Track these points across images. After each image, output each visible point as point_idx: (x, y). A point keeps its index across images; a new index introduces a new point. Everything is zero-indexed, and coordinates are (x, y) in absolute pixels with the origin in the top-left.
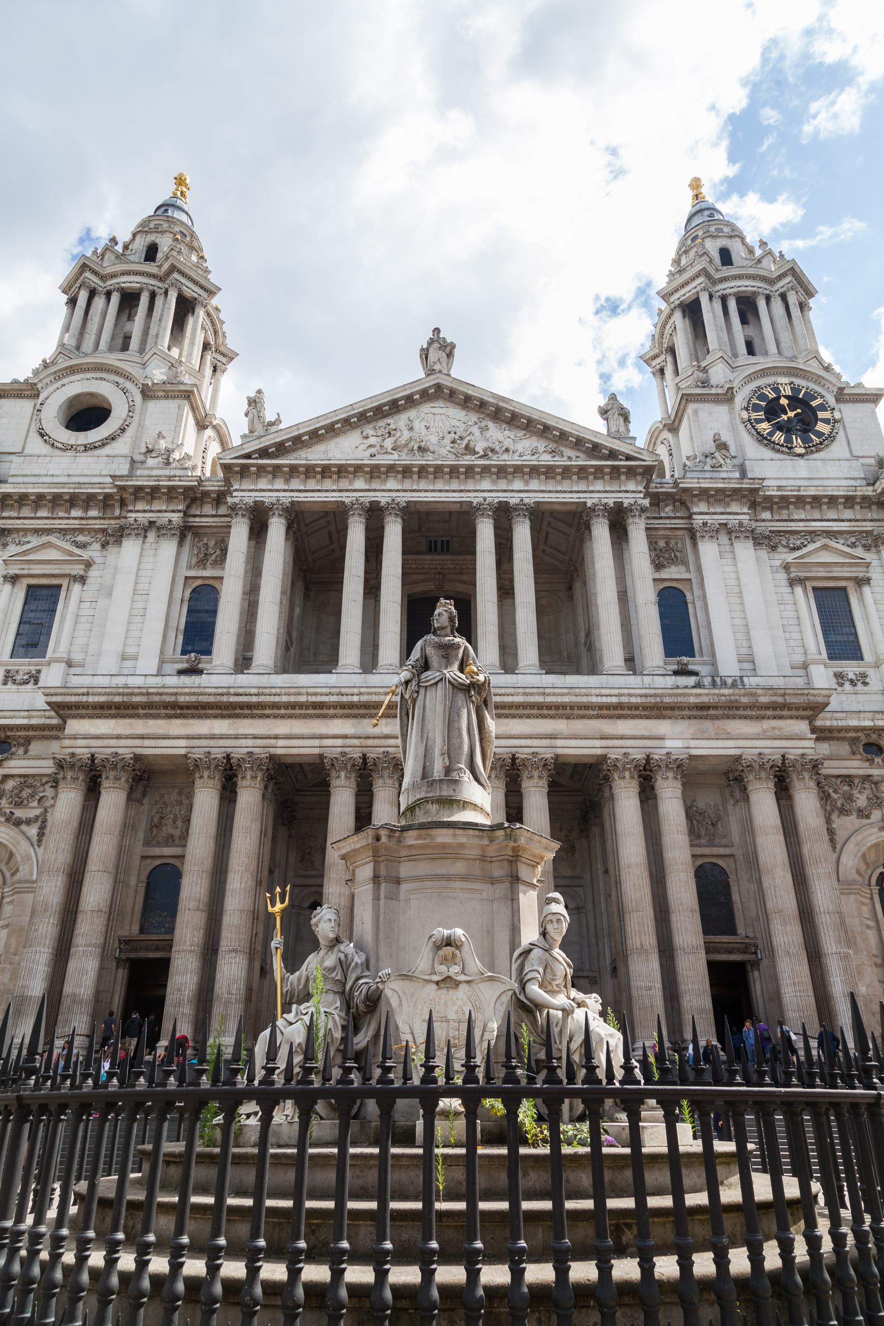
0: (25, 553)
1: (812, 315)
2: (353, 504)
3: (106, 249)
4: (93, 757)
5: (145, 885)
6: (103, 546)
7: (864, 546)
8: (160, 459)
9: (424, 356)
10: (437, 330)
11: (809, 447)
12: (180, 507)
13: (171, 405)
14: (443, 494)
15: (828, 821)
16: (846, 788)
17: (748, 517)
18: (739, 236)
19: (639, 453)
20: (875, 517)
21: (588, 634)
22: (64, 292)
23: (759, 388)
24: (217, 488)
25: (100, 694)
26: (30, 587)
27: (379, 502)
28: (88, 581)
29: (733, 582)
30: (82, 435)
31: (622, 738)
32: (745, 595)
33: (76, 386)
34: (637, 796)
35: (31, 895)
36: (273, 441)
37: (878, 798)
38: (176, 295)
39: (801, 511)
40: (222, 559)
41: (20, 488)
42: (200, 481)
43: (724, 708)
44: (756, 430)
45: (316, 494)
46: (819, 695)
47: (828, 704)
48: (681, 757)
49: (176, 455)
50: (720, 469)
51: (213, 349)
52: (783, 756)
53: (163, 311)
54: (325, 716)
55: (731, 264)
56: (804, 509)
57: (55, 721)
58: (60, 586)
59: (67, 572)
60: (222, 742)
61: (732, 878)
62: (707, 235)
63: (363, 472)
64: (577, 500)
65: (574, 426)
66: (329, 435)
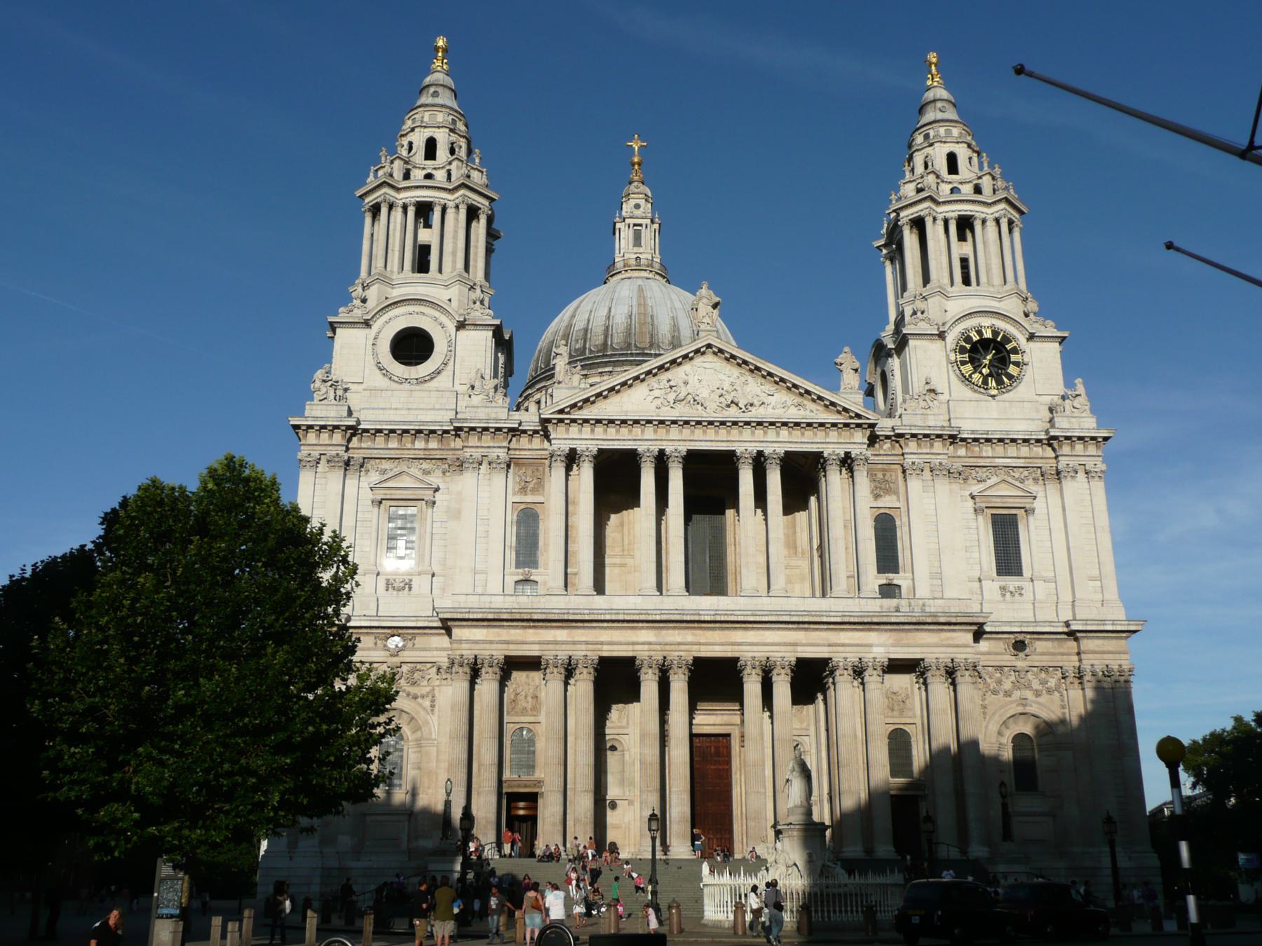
7: (1034, 479)
12: (505, 444)
14: (713, 444)
16: (998, 675)
17: (946, 457)
18: (965, 143)
24: (532, 428)
25: (477, 613)
30: (413, 368)
31: (843, 645)
33: (401, 320)
35: (435, 748)
36: (581, 398)
45: (616, 443)
48: (883, 660)
50: (928, 411)
52: (952, 660)
60: (564, 647)
61: (913, 739)
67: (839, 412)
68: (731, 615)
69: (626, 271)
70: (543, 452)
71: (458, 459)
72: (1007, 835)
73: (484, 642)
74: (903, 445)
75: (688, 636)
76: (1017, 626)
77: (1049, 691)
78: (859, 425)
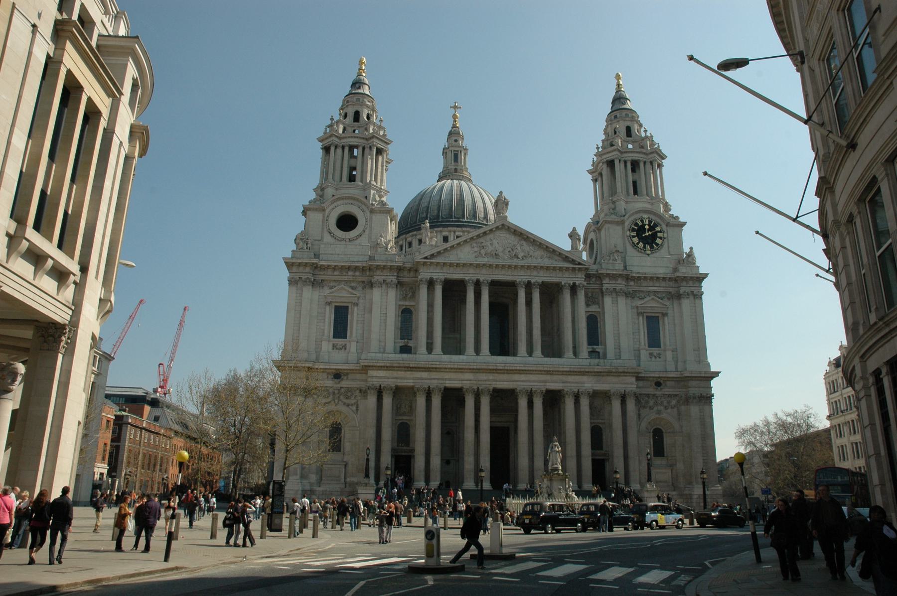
0: (332, 293)
1: (664, 169)
6: (363, 289)
7: (668, 298)
10: (501, 193)
14: (505, 276)
15: (639, 411)
22: (320, 141)
26: (336, 306)
28: (360, 305)
30: (347, 233)
31: (570, 383)
45: (454, 275)
54: (463, 372)
55: (631, 137)
60: (426, 381)
67: (569, 262)
69: (449, 176)
70: (416, 279)
71: (371, 281)
72: (649, 480)
73: (384, 377)
75: (491, 377)
78: (580, 269)
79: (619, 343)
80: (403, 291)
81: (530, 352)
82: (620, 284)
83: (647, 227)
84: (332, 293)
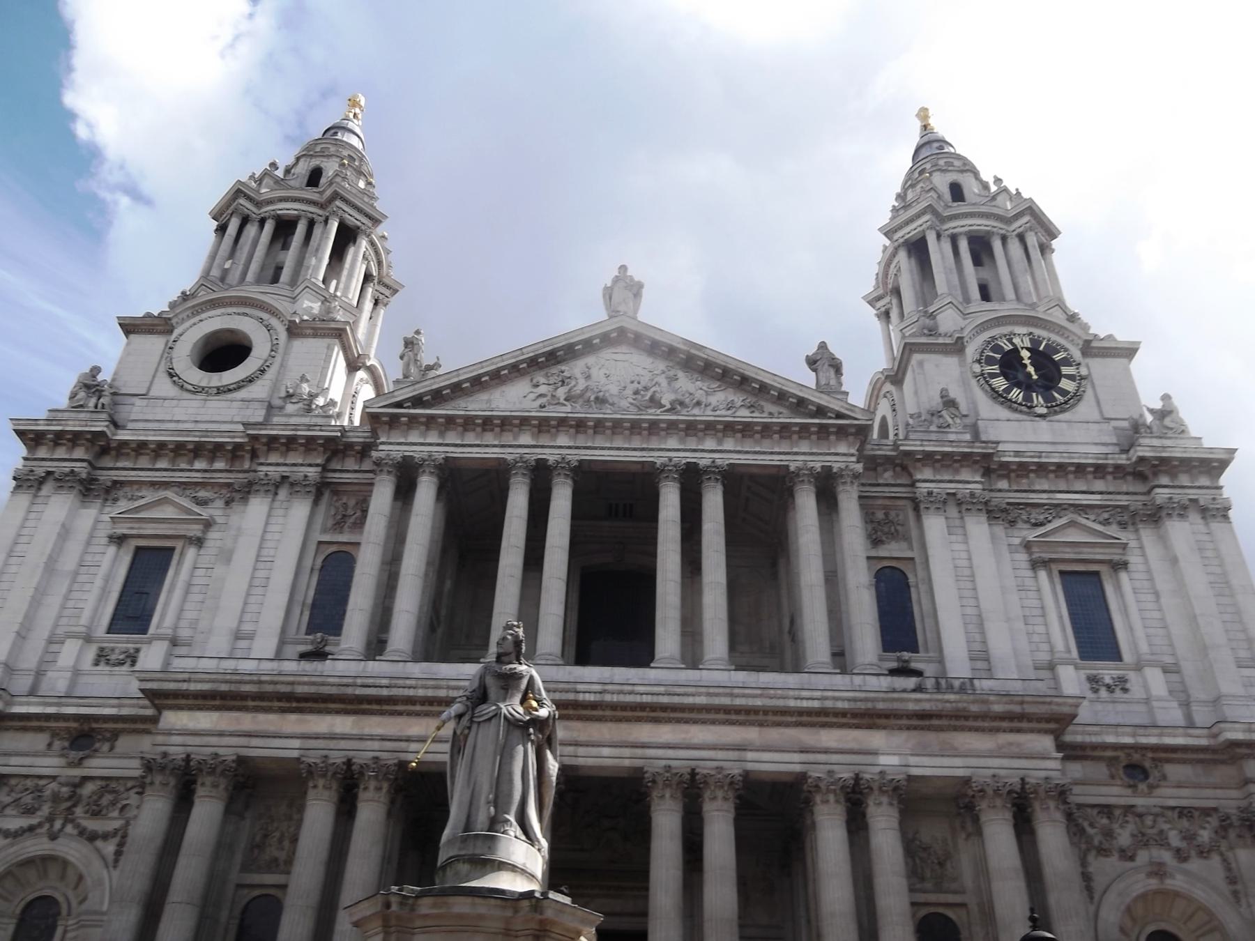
0: (137, 510)
1: (1056, 258)
2: (517, 462)
3: (266, 174)
4: (188, 758)
5: (237, 921)
6: (227, 503)
7: (1120, 523)
8: (300, 405)
9: (608, 297)
10: (623, 268)
11: (1052, 406)
12: (319, 461)
13: (320, 344)
15: (1084, 863)
16: (1105, 821)
17: (980, 486)
19: (852, 411)
20: (1131, 489)
21: (792, 622)
23: (993, 338)
26: (139, 550)
27: (546, 460)
28: (209, 544)
29: (965, 563)
32: (979, 580)
33: (215, 322)
34: (844, 825)
35: (99, 930)
37: (1143, 835)
38: (336, 224)
39: (1043, 481)
40: (360, 523)
41: (140, 435)
42: (343, 430)
43: (950, 717)
44: (990, 385)
46: (1064, 704)
47: (1074, 716)
48: (898, 777)
49: (320, 401)
51: (376, 281)
52: (1022, 779)
53: (321, 240)
56: (1046, 477)
57: (150, 712)
58: (172, 549)
59: (182, 533)
60: (343, 744)
62: (934, 169)
63: (530, 425)
64: (778, 463)
65: (776, 378)
66: (493, 382)
68: (630, 693)
74: (912, 471)
76: (1128, 735)
77: (1203, 853)
79: (984, 642)
80: (337, 508)
81: (692, 656)
82: (971, 482)
83: (1025, 354)
84: (137, 510)
